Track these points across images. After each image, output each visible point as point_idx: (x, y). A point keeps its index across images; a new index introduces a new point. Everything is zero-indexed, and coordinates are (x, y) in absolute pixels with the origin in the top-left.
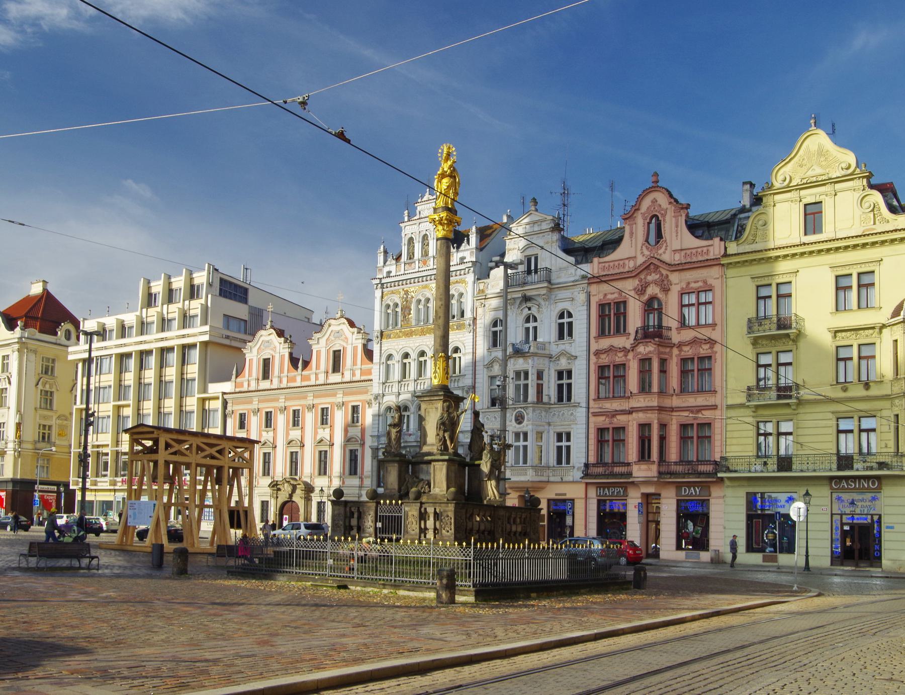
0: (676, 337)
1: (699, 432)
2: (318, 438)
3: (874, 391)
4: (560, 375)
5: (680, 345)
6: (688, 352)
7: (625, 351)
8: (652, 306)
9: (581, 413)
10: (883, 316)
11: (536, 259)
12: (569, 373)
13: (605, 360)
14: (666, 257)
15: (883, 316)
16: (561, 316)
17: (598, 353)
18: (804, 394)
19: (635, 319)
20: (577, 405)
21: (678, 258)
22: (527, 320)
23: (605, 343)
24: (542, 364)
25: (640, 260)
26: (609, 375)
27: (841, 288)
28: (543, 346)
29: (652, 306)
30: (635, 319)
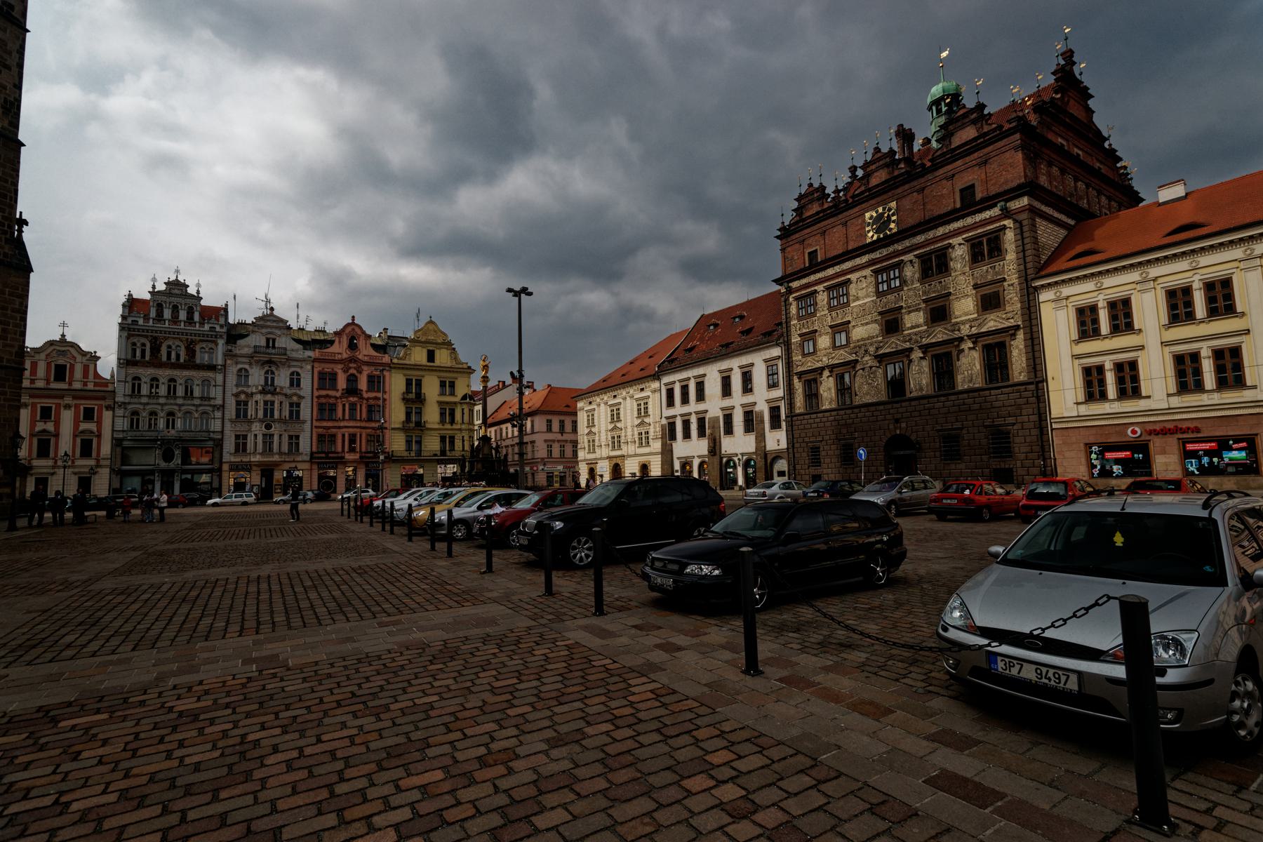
0: (365, 395)
1: (377, 438)
2: (37, 429)
3: (455, 426)
4: (291, 405)
5: (368, 399)
6: (372, 402)
7: (336, 398)
8: (352, 380)
9: (307, 426)
10: (457, 399)
11: (274, 340)
12: (298, 405)
13: (323, 400)
14: (360, 357)
15: (457, 399)
16: (292, 374)
17: (318, 397)
18: (428, 426)
19: (342, 383)
20: (304, 422)
21: (366, 359)
22: (267, 372)
23: (323, 393)
24: (282, 398)
25: (345, 356)
26: (325, 410)
27: (443, 384)
28: (282, 388)
29: (352, 380)
30: (342, 383)
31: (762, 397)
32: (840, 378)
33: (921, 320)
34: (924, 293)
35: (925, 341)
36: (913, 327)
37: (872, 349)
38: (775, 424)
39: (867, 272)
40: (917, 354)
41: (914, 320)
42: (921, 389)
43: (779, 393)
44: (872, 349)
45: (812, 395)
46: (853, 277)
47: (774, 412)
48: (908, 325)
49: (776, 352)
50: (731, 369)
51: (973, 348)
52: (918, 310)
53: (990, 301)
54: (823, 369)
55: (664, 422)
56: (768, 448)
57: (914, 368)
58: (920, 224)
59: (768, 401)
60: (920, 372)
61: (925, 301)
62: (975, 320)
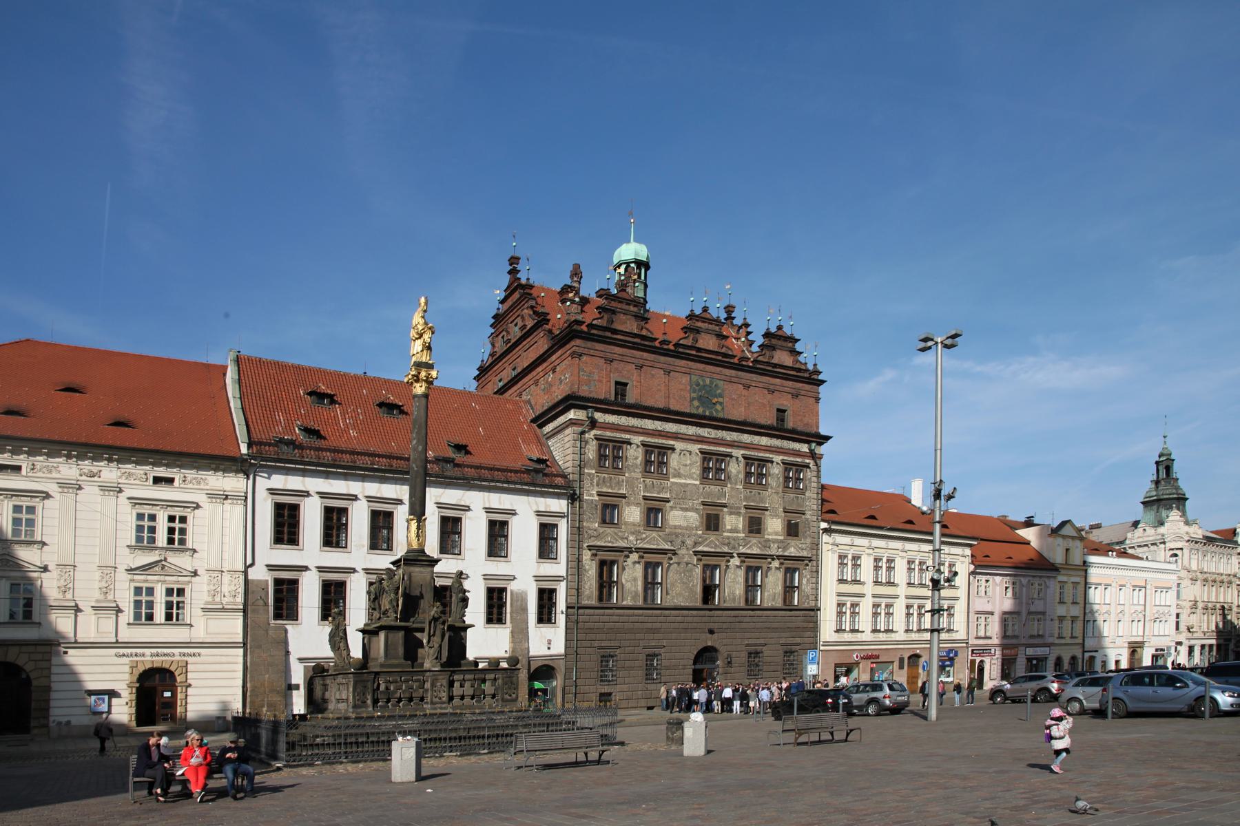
31: (524, 569)
32: (650, 567)
33: (741, 526)
34: (746, 498)
35: (742, 550)
36: (731, 531)
37: (689, 542)
38: (545, 614)
39: (696, 448)
40: (736, 561)
41: (733, 522)
42: (734, 600)
43: (559, 568)
44: (689, 542)
45: (605, 584)
46: (679, 445)
47: (546, 598)
48: (728, 527)
49: (559, 505)
50: (467, 509)
51: (739, 567)
52: (738, 514)
53: (792, 530)
54: (630, 550)
55: (259, 573)
56: (531, 654)
57: (730, 575)
58: (744, 423)
59: (538, 579)
60: (734, 581)
61: (746, 508)
62: (781, 541)
